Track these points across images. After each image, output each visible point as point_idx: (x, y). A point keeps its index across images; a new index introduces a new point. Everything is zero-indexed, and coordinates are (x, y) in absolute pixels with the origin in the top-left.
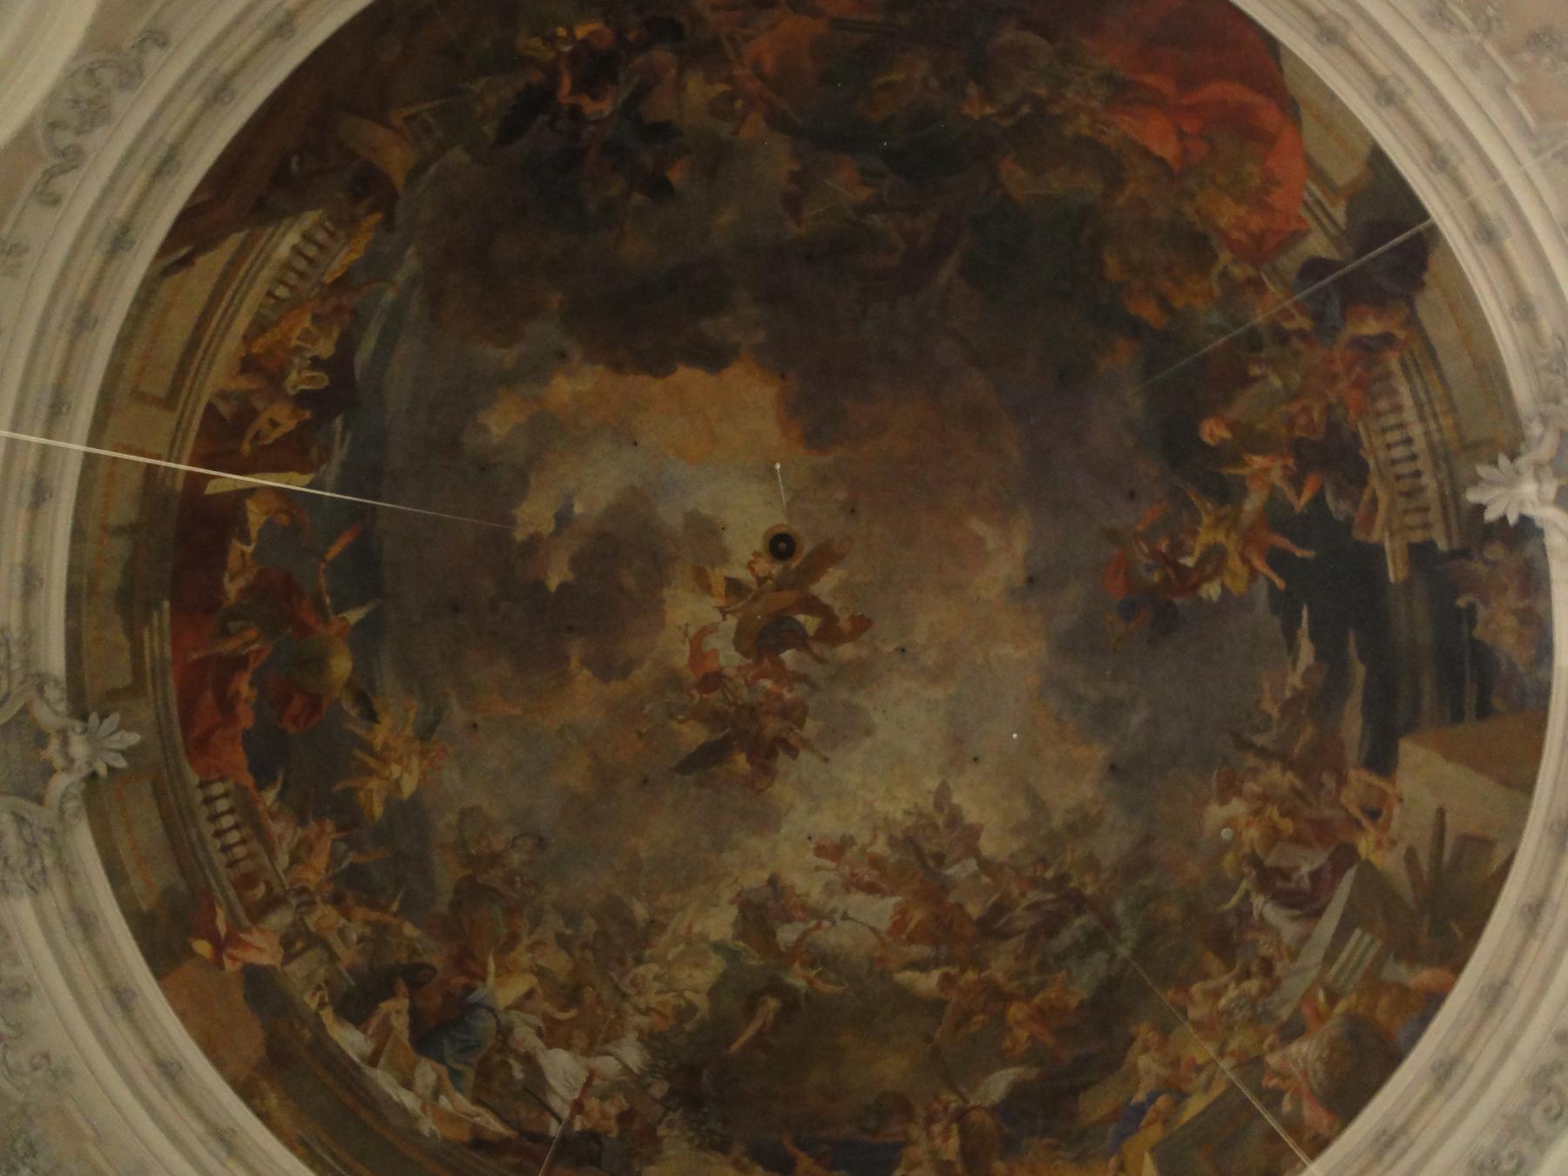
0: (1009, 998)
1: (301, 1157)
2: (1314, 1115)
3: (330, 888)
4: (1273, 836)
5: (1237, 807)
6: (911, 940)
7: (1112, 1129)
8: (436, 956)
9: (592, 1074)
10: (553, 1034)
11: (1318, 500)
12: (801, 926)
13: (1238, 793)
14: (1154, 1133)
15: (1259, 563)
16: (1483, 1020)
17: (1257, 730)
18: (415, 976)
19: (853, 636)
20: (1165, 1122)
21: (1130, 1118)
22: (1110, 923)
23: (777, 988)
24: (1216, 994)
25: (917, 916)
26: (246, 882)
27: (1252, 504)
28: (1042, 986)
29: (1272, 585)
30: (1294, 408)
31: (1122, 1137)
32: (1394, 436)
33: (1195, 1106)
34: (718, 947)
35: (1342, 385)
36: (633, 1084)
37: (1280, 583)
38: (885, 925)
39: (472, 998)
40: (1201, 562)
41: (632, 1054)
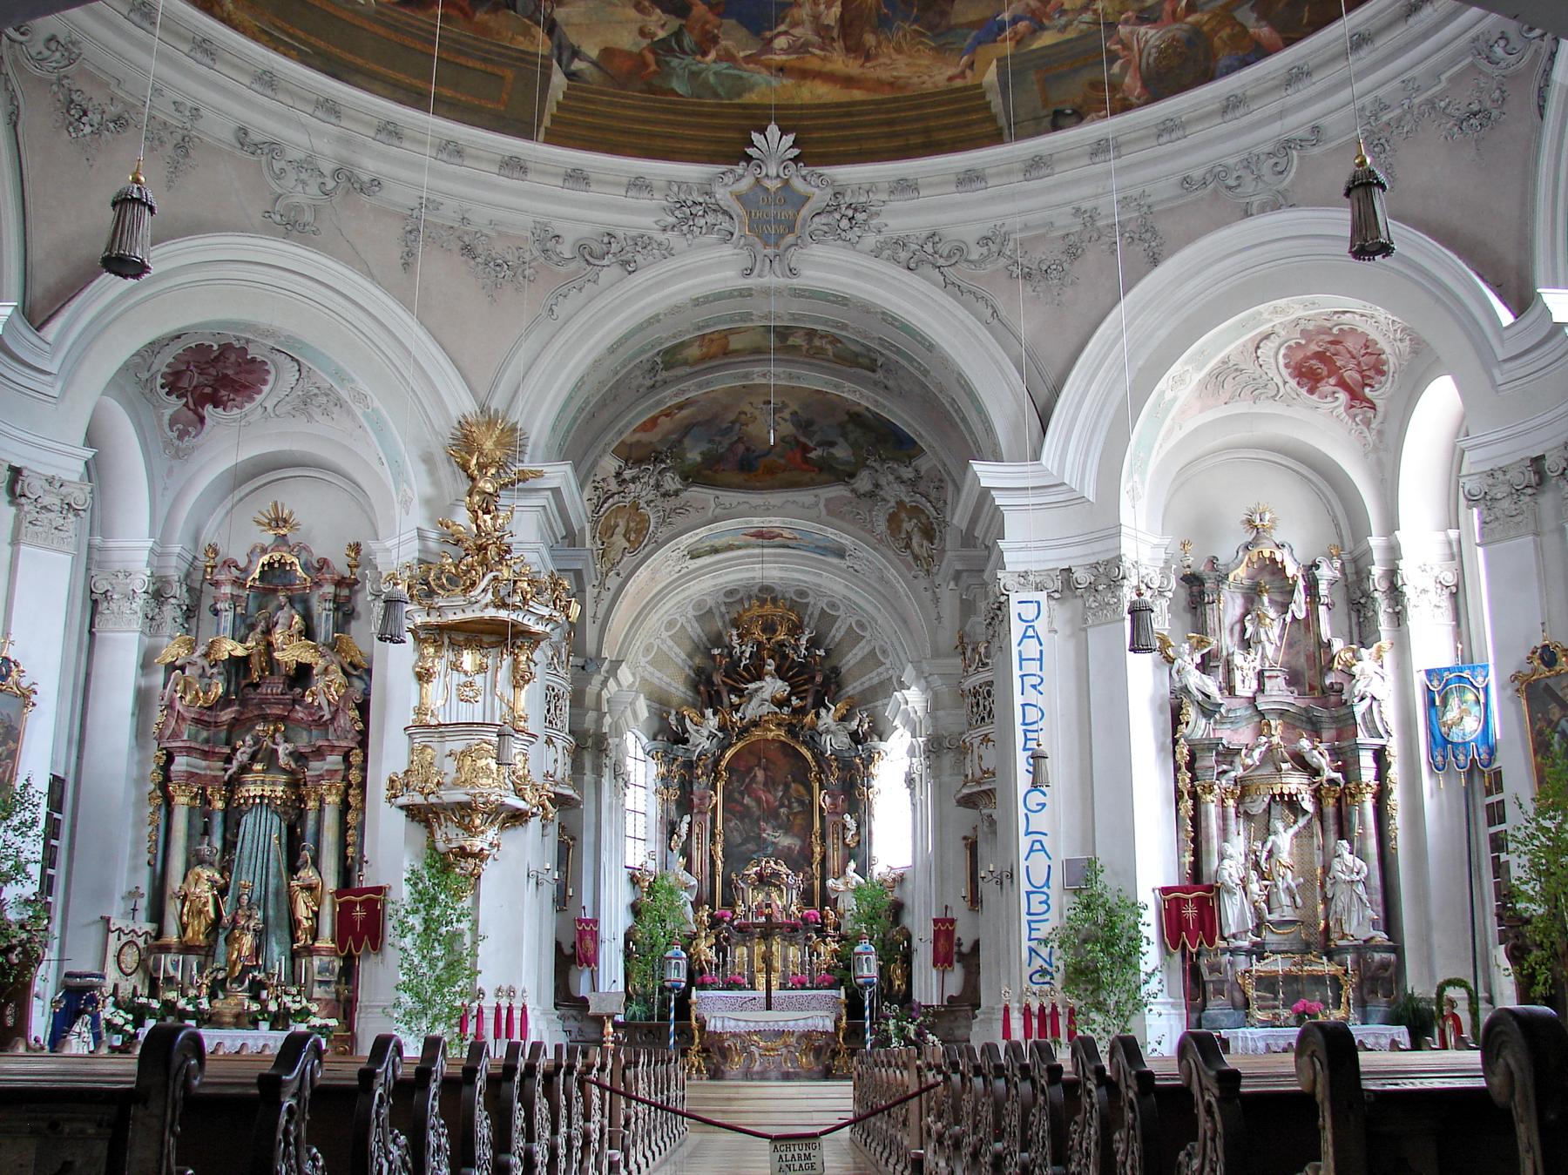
1: (266, 45)
2: (1132, 84)
7: (974, 33)
14: (1008, 48)
16: (1277, 88)
20: (1018, 43)
31: (979, 42)
33: (1047, 39)
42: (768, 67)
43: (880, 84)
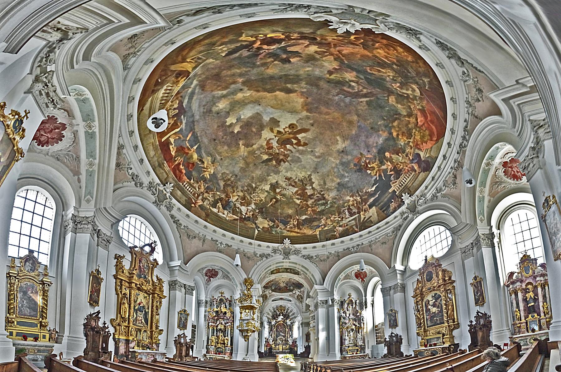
0: (309, 207)
3: (205, 191)
4: (353, 205)
5: (351, 199)
6: (297, 195)
8: (223, 196)
9: (248, 209)
10: (242, 204)
11: (392, 175)
12: (280, 190)
13: (353, 197)
15: (378, 174)
17: (360, 192)
18: (221, 199)
19: (303, 146)
21: (318, 227)
22: (327, 203)
23: (275, 198)
24: (335, 218)
25: (300, 192)
26: (194, 195)
27: (384, 167)
28: (314, 207)
29: (377, 178)
30: (399, 163)
31: (317, 228)
32: (405, 179)
33: (326, 228)
34: (267, 191)
35: (407, 168)
36: (254, 210)
37: (378, 179)
38: (294, 192)
39: (230, 201)
40: (371, 167)
41: (253, 206)
42: (286, 230)
43: (302, 233)
